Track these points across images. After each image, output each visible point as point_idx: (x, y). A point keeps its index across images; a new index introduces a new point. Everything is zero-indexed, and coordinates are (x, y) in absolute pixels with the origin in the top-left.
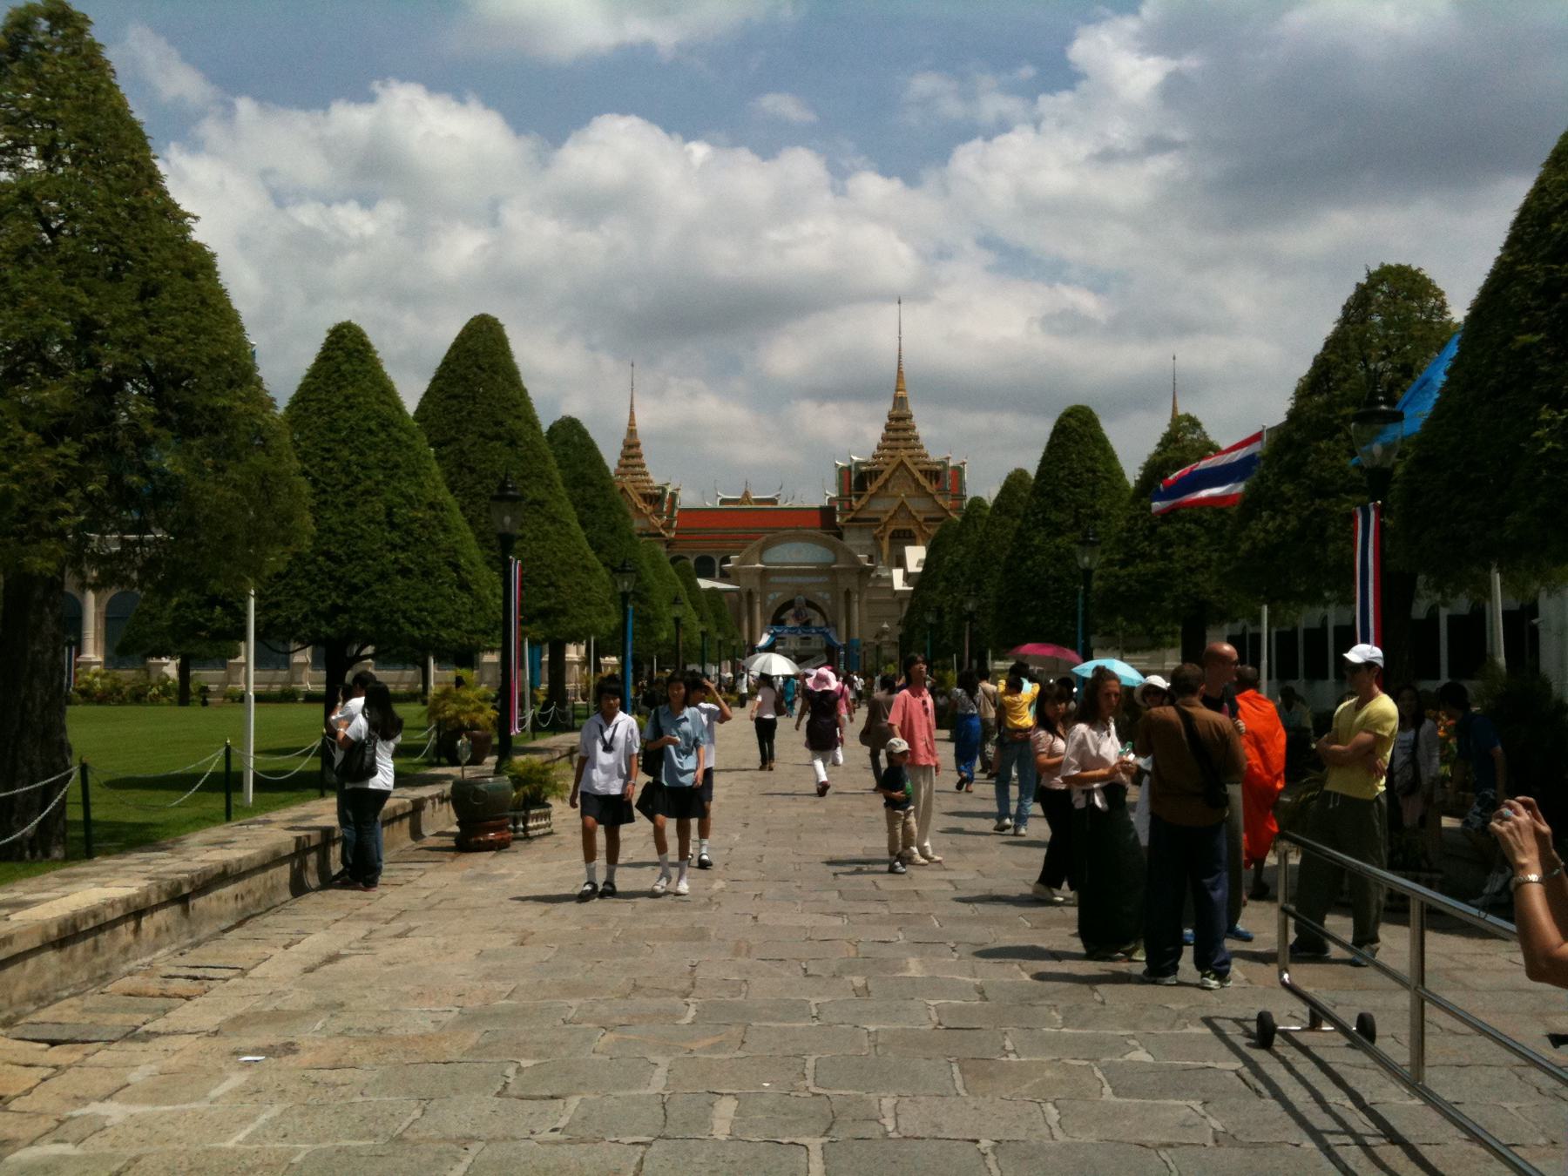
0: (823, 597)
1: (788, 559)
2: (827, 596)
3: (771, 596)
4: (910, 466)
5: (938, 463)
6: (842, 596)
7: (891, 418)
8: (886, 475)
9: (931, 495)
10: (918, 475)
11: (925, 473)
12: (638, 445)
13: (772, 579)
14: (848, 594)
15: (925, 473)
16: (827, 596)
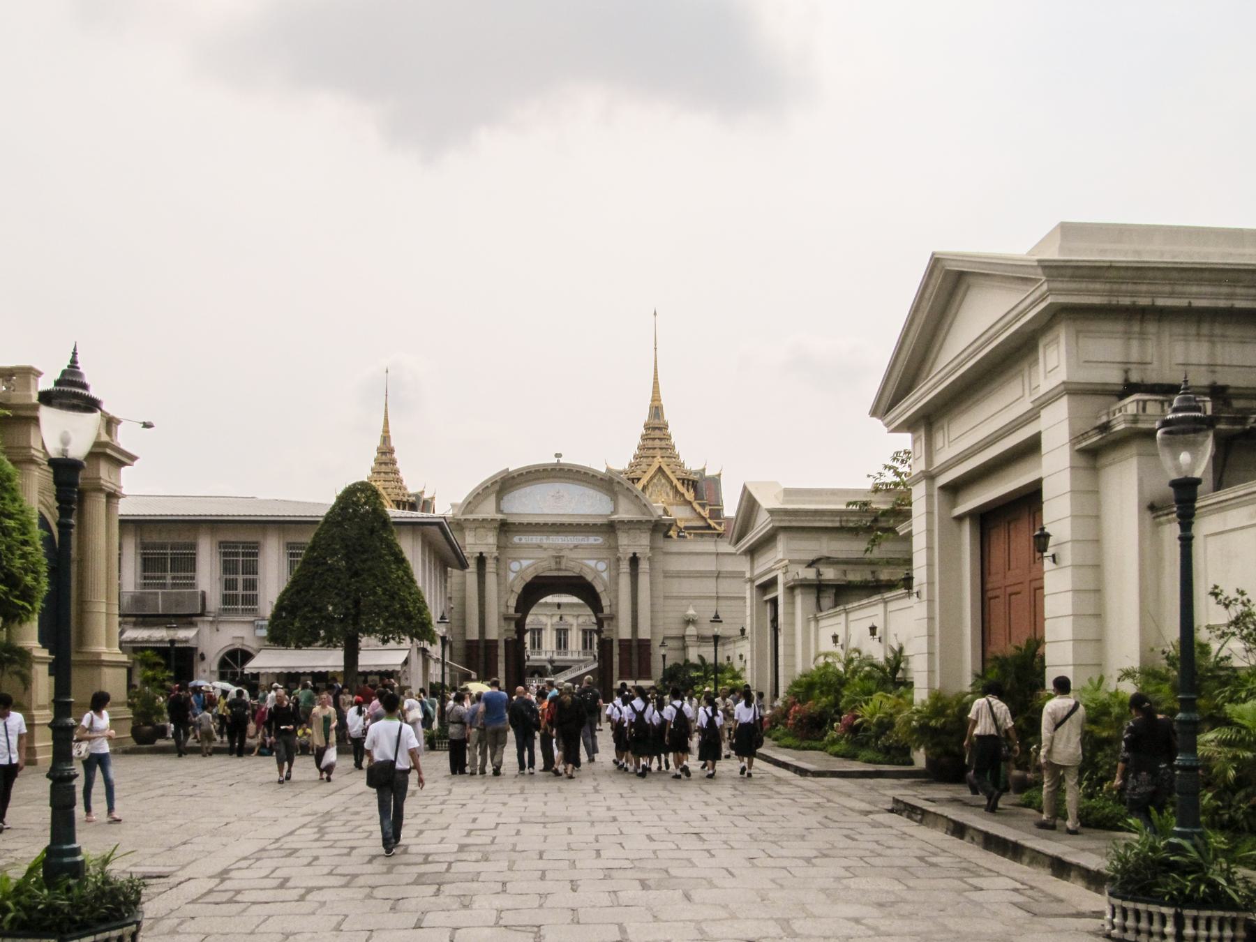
0: (595, 568)
1: (546, 511)
2: (602, 566)
3: (515, 566)
4: (668, 472)
5: (695, 473)
6: (625, 567)
7: (647, 427)
8: (644, 481)
9: (690, 503)
10: (675, 482)
11: (683, 481)
12: (392, 451)
13: (516, 539)
14: (634, 561)
15: (683, 481)
16: (602, 566)
